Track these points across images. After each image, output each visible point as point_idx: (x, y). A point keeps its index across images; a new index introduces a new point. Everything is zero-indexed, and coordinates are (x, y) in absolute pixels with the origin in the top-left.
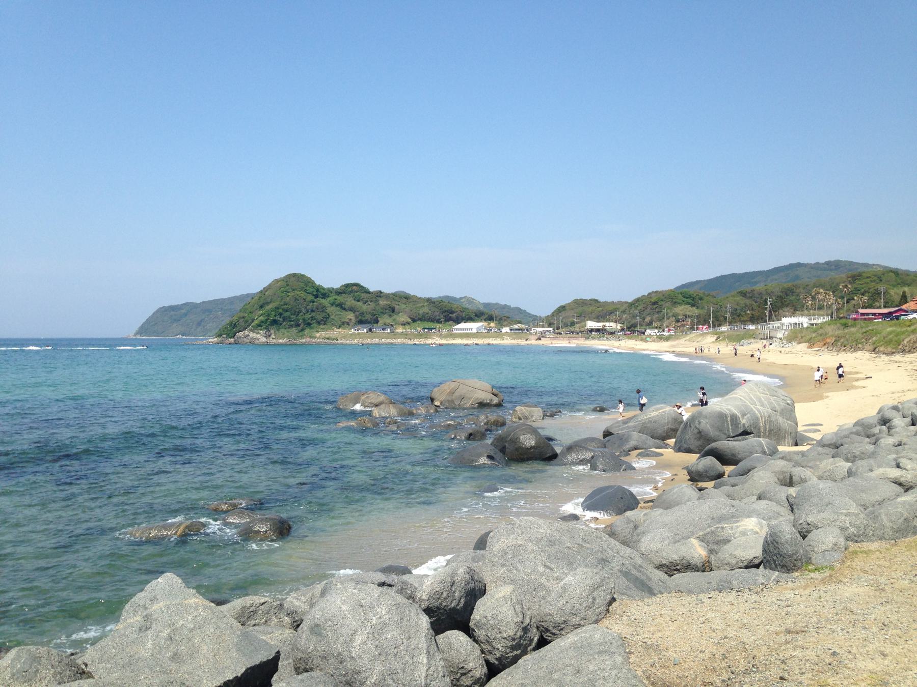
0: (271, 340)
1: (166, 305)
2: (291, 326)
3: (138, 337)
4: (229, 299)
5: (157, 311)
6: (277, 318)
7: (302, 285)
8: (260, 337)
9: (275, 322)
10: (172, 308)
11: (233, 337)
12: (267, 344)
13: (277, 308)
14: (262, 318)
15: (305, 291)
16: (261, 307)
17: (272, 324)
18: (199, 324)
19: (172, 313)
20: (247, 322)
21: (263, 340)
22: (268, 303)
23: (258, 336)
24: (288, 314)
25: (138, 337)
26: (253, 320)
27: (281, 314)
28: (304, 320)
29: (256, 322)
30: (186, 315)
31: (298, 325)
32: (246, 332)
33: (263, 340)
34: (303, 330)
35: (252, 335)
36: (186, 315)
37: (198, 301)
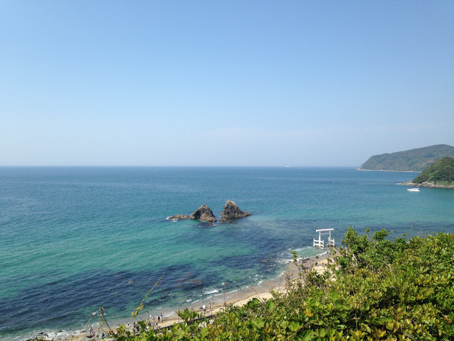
0: (437, 186)
1: (376, 154)
2: (445, 180)
3: (363, 170)
4: (406, 151)
5: (371, 158)
6: (439, 177)
7: (450, 162)
8: (432, 184)
9: (438, 178)
10: (378, 156)
11: (421, 183)
12: (435, 188)
13: (439, 172)
14: (432, 177)
15: (452, 165)
16: (432, 172)
17: (437, 179)
18: (391, 165)
19: (378, 159)
20: (426, 177)
21: (433, 185)
22: (435, 170)
23: (431, 184)
24: (444, 175)
25: (363, 170)
26: (429, 177)
27: (441, 175)
28: (451, 177)
29: (430, 178)
30: (384, 159)
31: (448, 180)
32: (426, 182)
33: (433, 185)
34: (451, 182)
35: (428, 183)
36: (384, 159)
37: (390, 152)
